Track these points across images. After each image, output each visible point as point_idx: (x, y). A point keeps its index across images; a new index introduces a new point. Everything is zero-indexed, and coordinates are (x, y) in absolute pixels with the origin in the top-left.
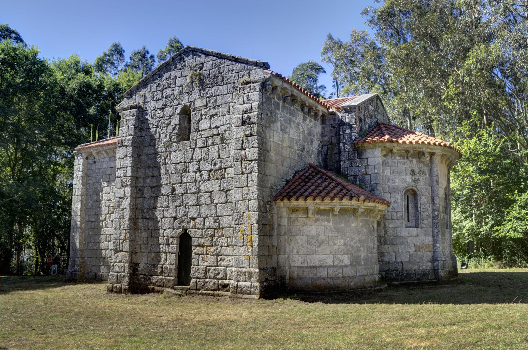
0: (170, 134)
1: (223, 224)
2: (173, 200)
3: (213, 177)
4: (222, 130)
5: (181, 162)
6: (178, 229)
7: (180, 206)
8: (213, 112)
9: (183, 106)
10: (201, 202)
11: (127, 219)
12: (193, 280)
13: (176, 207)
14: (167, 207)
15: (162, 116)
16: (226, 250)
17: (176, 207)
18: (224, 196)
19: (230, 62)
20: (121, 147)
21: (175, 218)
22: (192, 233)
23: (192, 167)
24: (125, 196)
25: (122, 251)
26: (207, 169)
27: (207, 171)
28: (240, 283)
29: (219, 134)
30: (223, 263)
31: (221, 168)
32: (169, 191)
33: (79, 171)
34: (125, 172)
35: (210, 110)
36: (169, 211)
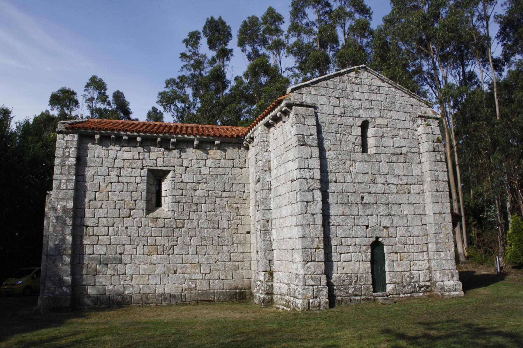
0: (353, 143)
1: (414, 233)
2: (364, 208)
3: (401, 190)
4: (404, 150)
5: (368, 173)
6: (371, 237)
7: (372, 215)
8: (395, 132)
9: (364, 120)
10: (393, 213)
11: (320, 226)
12: (389, 288)
13: (368, 215)
14: (358, 215)
15: (341, 123)
16: (418, 256)
17: (368, 215)
18: (413, 208)
19: (404, 94)
20: (303, 145)
21: (367, 227)
22: (385, 241)
23: (380, 180)
24: (314, 200)
25: (314, 261)
26: (395, 183)
27: (395, 184)
28: (445, 283)
29: (401, 154)
30: (416, 268)
31: (407, 184)
32: (359, 200)
33: (69, 156)
34: (312, 173)
35: (391, 130)
36: (361, 220)
